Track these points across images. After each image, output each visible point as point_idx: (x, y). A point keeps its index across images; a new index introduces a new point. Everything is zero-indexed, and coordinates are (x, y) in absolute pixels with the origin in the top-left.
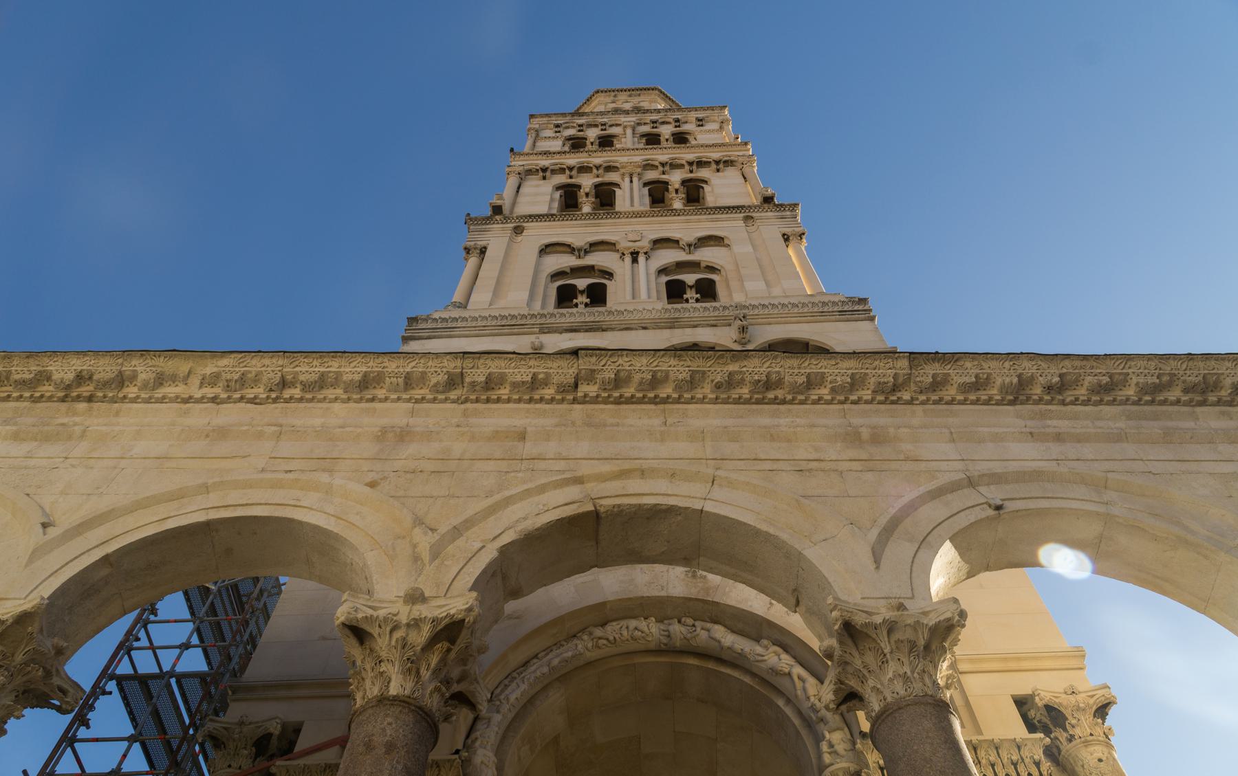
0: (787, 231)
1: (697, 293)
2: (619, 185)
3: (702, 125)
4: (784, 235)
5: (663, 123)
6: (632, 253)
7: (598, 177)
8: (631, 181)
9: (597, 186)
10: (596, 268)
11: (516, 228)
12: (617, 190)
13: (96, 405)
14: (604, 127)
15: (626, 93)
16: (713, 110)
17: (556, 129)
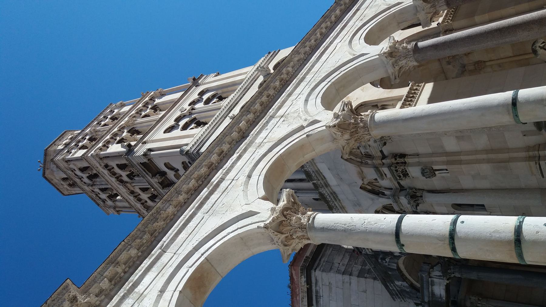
2: (134, 127)
6: (192, 110)
10: (188, 122)
11: (142, 144)
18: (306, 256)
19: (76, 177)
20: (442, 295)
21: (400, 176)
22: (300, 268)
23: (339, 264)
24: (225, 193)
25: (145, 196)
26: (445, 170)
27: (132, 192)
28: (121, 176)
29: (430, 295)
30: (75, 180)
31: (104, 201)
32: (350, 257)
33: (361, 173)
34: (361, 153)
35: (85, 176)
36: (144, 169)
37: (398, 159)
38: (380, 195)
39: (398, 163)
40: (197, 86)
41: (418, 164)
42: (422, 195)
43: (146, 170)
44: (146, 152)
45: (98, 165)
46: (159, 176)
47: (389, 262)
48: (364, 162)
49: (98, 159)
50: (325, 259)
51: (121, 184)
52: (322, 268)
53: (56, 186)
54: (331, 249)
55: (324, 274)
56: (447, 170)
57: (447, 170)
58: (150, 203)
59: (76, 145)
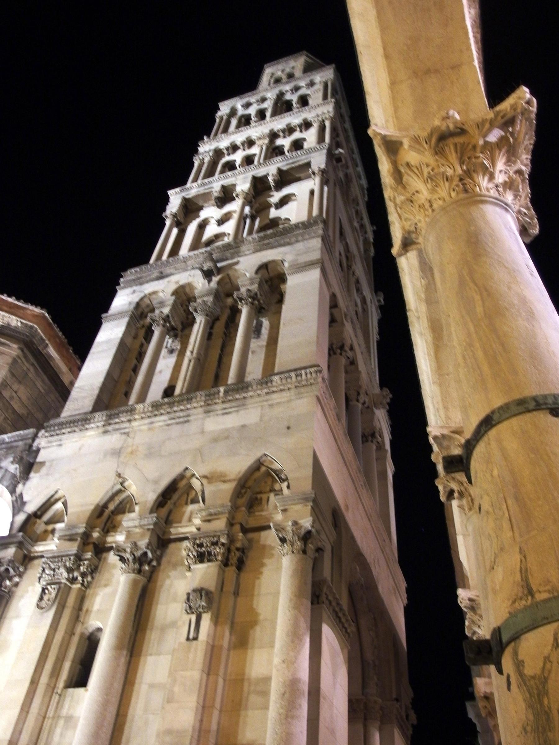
18: (49, 345)
22: (35, 326)
23: (16, 392)
25: (238, 157)
26: (195, 636)
32: (19, 415)
33: (223, 479)
34: (261, 493)
36: (297, 164)
37: (238, 554)
43: (293, 165)
47: (6, 470)
48: (243, 491)
50: (31, 373)
52: (19, 361)
54: (42, 391)
55: (10, 360)
56: (195, 638)
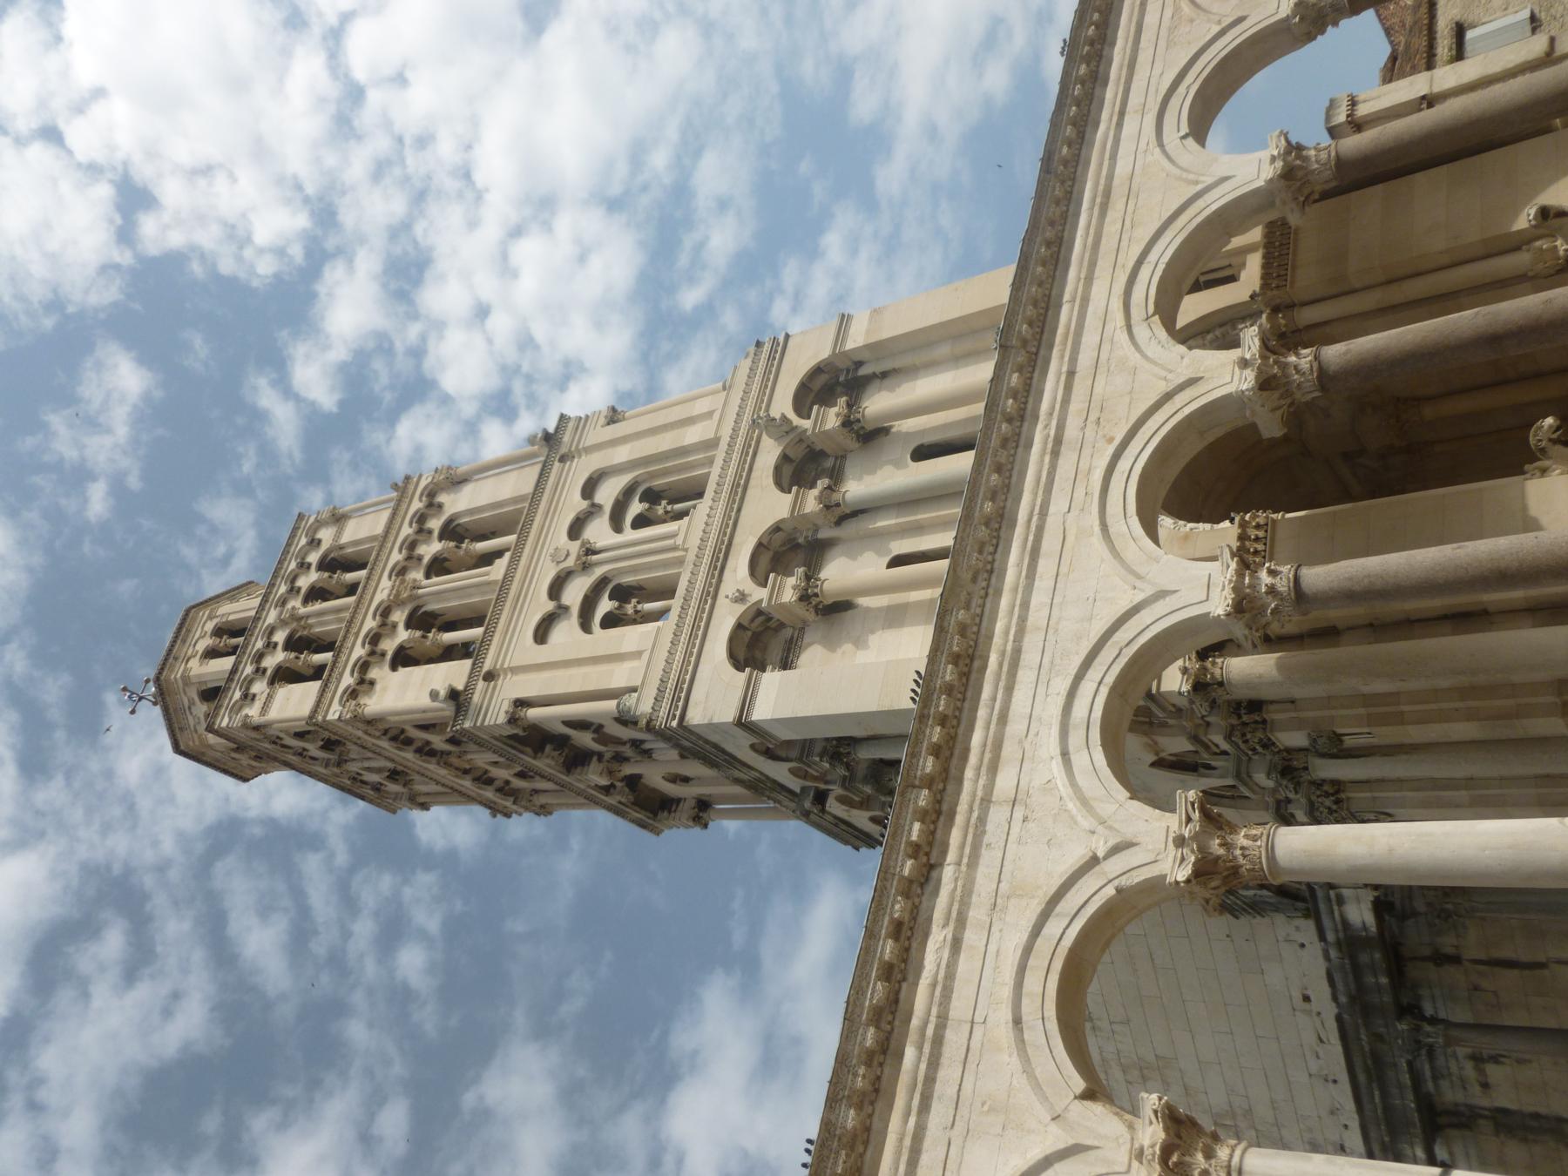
0: (602, 420)
1: (660, 505)
3: (320, 541)
4: (608, 424)
5: (293, 580)
6: (587, 554)
7: (395, 626)
8: (425, 588)
9: (408, 626)
11: (485, 679)
12: (423, 610)
13: (978, 653)
14: (272, 645)
15: (177, 647)
16: (299, 528)
17: (249, 698)
19: (286, 753)
20: (1366, 921)
21: (1254, 750)
24: (971, 1066)
27: (466, 772)
28: (428, 743)
29: (1340, 927)
30: (283, 758)
31: (377, 788)
35: (313, 749)
38: (1202, 770)
39: (1245, 724)
40: (562, 459)
41: (1298, 724)
42: (1306, 765)
44: (514, 713)
45: (360, 733)
46: (554, 750)
49: (362, 725)
51: (434, 760)
53: (216, 764)
56: (1369, 734)
57: (1369, 734)
58: (518, 783)
59: (257, 670)
